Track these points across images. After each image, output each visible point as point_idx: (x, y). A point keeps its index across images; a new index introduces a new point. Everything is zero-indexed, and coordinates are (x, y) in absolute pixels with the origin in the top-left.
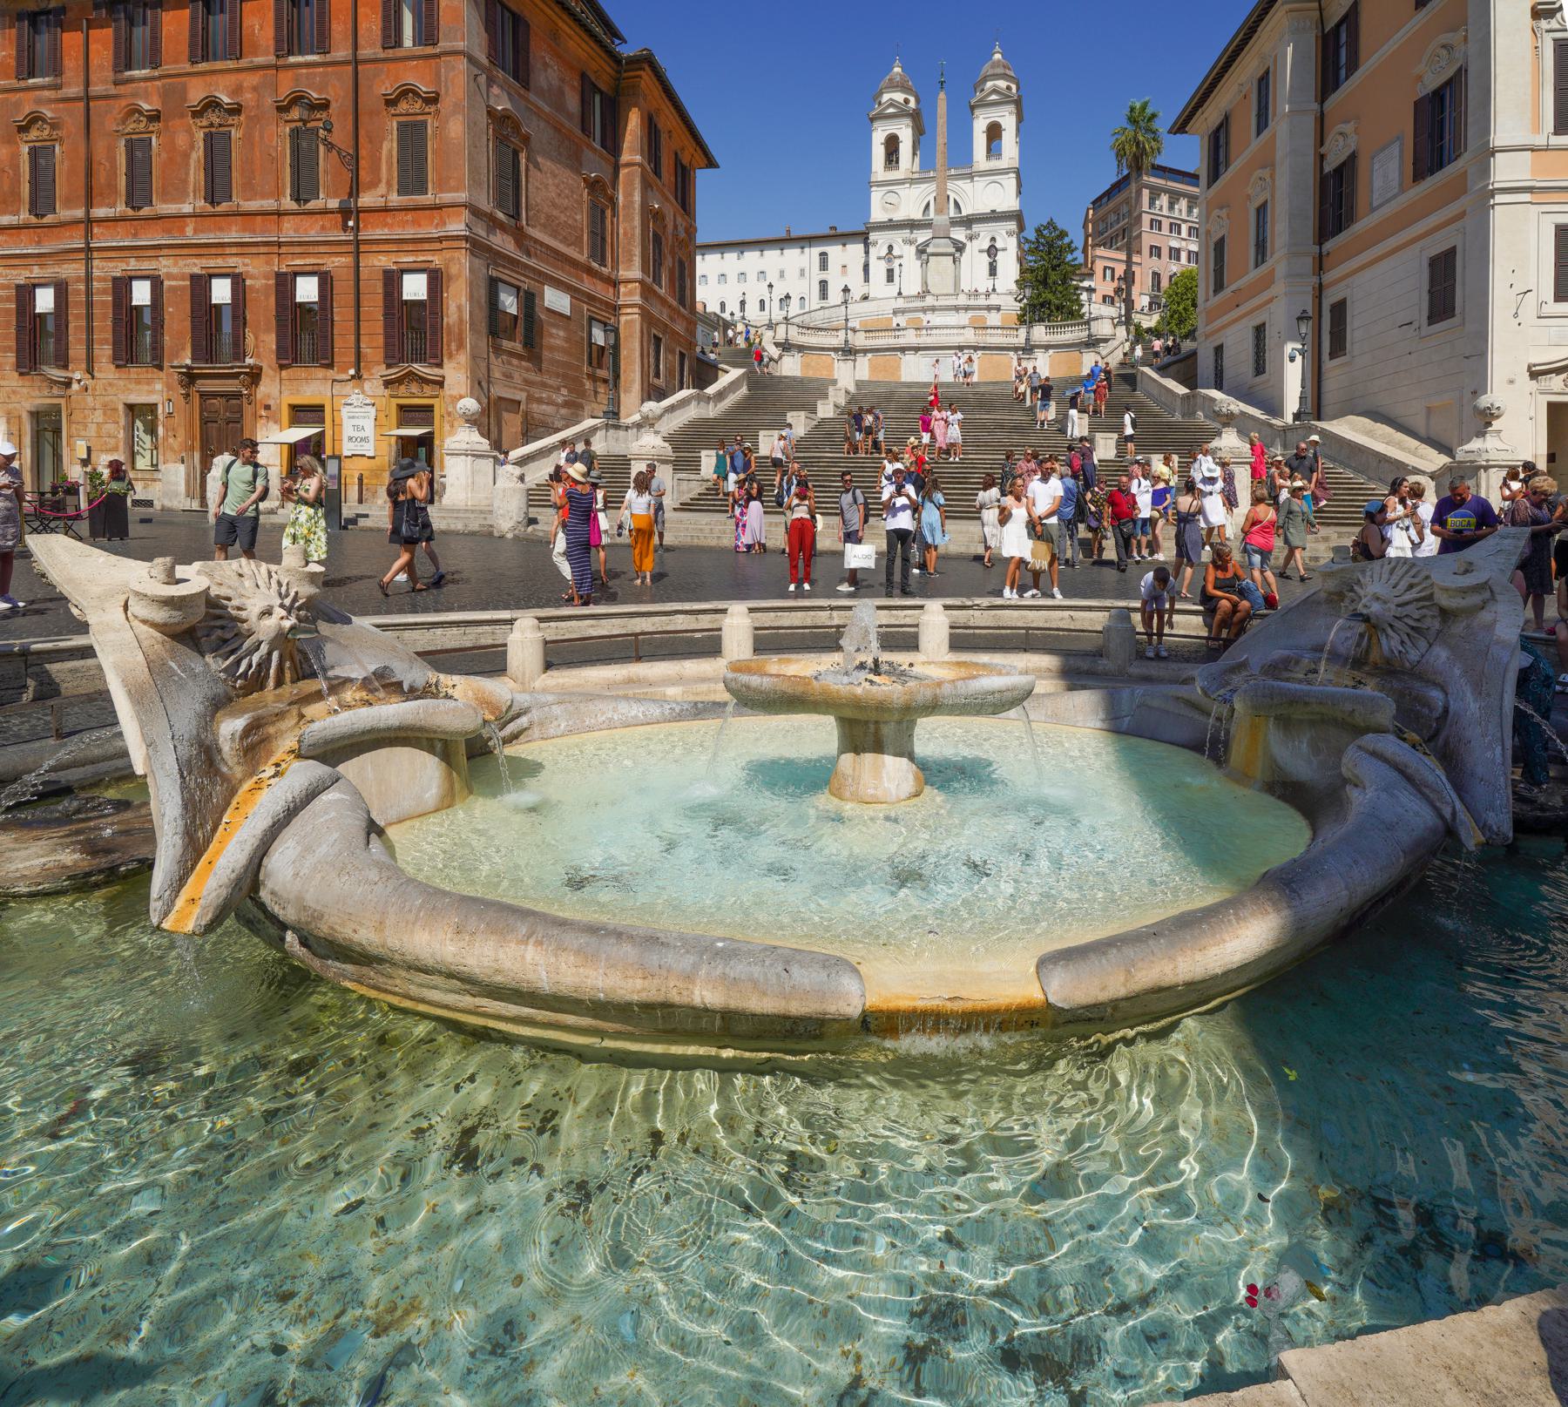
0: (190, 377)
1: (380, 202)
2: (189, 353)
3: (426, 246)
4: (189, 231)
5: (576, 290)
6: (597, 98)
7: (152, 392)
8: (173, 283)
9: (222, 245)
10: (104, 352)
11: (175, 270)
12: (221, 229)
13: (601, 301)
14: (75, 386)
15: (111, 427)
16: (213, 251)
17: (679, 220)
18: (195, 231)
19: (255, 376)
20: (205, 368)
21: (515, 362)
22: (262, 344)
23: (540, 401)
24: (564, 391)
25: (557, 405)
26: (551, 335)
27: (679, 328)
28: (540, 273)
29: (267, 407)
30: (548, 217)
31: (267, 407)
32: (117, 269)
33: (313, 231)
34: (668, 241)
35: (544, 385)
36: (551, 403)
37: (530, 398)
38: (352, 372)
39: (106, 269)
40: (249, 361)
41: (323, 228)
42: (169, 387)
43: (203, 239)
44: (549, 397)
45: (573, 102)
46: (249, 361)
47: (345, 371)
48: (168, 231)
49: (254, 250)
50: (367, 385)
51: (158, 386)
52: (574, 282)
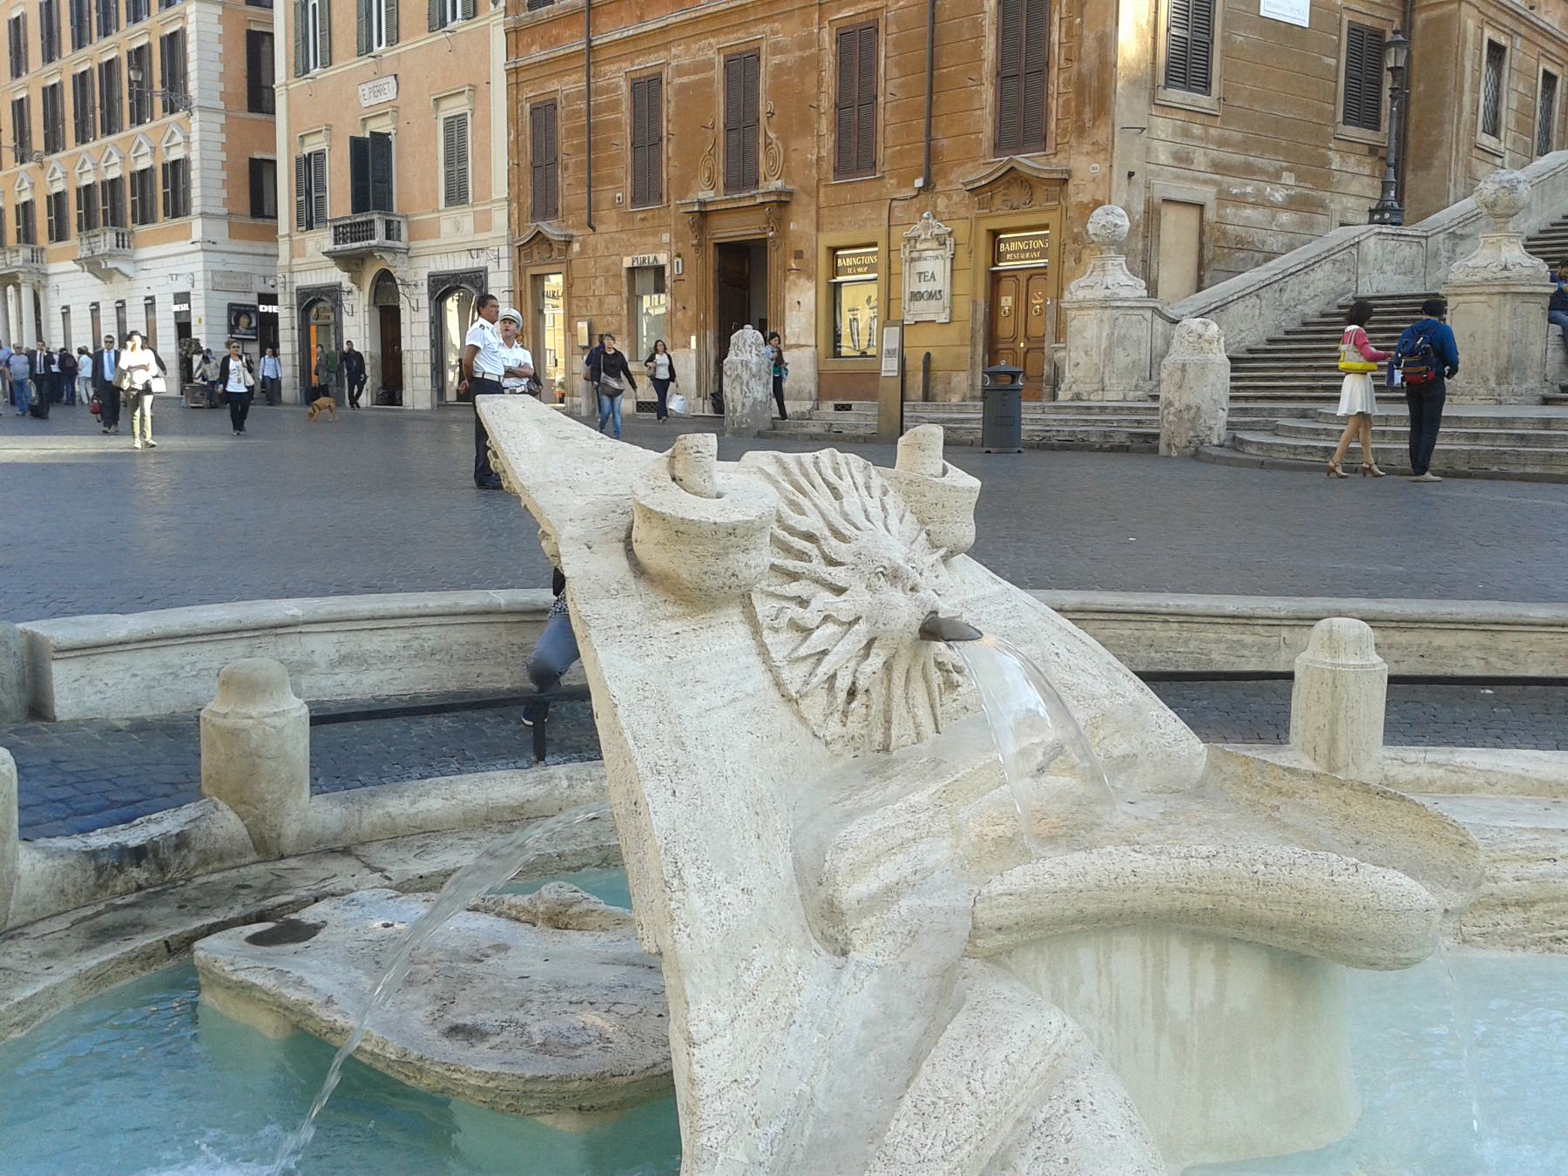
7: (658, 247)
8: (685, 79)
14: (576, 247)
19: (782, 203)
24: (1289, 178)
29: (799, 255)
31: (799, 255)
42: (678, 237)
46: (776, 184)
47: (906, 181)
50: (941, 203)
51: (666, 238)
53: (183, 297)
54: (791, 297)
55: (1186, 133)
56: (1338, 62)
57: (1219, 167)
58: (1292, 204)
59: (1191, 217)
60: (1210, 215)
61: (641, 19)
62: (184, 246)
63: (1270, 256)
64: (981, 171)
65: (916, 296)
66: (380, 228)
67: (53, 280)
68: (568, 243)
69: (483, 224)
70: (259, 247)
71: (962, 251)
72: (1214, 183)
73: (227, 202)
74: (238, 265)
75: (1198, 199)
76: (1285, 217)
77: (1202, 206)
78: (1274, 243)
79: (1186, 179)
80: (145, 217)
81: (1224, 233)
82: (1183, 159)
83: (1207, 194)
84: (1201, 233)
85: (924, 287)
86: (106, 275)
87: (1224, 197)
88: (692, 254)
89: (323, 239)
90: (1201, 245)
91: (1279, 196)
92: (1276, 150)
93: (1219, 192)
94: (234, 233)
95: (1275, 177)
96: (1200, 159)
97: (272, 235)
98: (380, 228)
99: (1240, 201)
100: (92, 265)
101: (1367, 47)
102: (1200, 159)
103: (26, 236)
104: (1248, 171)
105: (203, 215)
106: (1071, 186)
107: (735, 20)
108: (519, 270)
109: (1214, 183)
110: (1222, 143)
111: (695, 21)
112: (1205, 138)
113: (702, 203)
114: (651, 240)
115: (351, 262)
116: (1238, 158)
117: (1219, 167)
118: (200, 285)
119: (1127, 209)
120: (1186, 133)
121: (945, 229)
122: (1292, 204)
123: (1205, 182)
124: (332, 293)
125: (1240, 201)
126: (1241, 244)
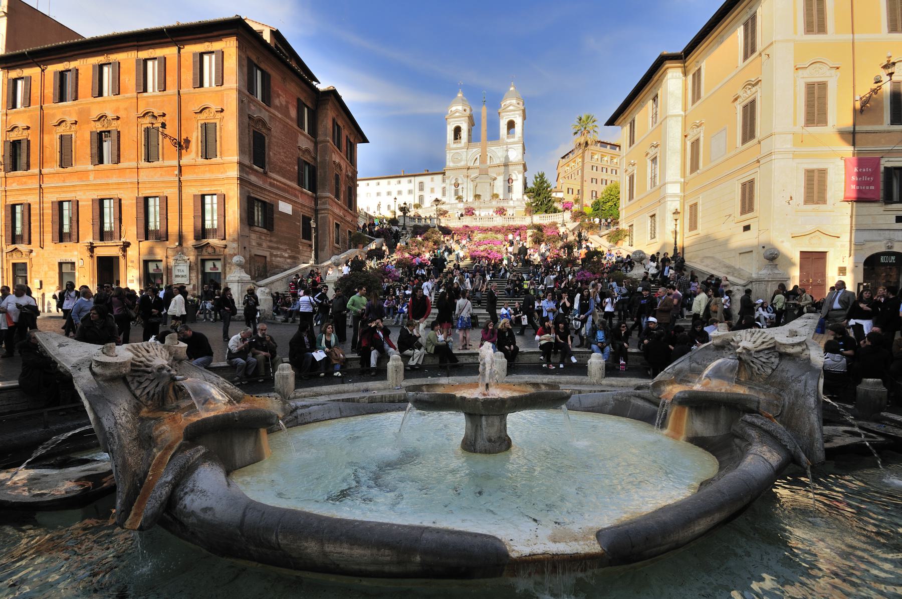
1: (193, 162)
3: (216, 183)
4: (91, 177)
5: (295, 202)
6: (306, 110)
9: (108, 184)
10: (48, 237)
11: (84, 197)
12: (108, 177)
13: (308, 207)
16: (104, 187)
17: (349, 168)
18: (95, 178)
22: (131, 231)
27: (349, 219)
28: (276, 194)
30: (281, 167)
32: (56, 197)
33: (157, 176)
34: (342, 178)
38: (177, 244)
39: (51, 197)
41: (161, 175)
43: (99, 182)
45: (293, 113)
48: (81, 179)
49: (125, 186)
52: (294, 199)
55: (260, 238)
56: (300, 224)
57: (270, 247)
58: (290, 257)
60: (268, 259)
63: (285, 270)
65: (177, 276)
76: (289, 261)
77: (265, 257)
78: (286, 267)
82: (260, 245)
83: (267, 254)
85: (180, 274)
87: (272, 255)
91: (287, 255)
92: (285, 244)
95: (285, 251)
99: (276, 256)
101: (306, 220)
102: (265, 245)
104: (278, 249)
110: (271, 241)
116: (276, 245)
117: (270, 247)
119: (244, 257)
120: (260, 238)
122: (290, 257)
125: (276, 256)
126: (277, 267)
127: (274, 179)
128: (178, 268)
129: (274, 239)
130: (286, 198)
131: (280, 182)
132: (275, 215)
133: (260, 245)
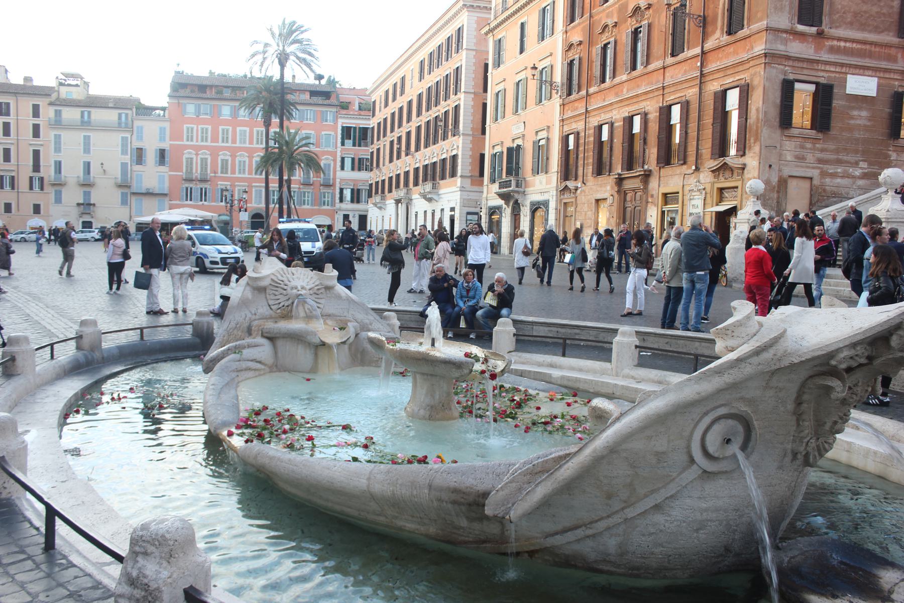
0: (620, 180)
2: (620, 167)
7: (605, 191)
14: (579, 191)
15: (589, 213)
20: (626, 174)
21: (809, 145)
23: (834, 175)
25: (854, 177)
26: (852, 118)
28: (842, 65)
35: (839, 162)
36: (846, 176)
37: (824, 174)
40: (646, 167)
42: (612, 188)
44: (845, 172)
46: (646, 167)
51: (609, 188)
53: (453, 209)
54: (649, 213)
55: (802, 147)
59: (806, 185)
60: (816, 182)
61: (604, 100)
62: (454, 189)
64: (714, 164)
66: (513, 183)
67: (414, 201)
68: (576, 190)
69: (549, 182)
70: (476, 188)
71: (708, 196)
72: (819, 168)
73: (471, 171)
74: (473, 196)
75: (809, 175)
77: (811, 179)
79: (802, 167)
80: (443, 177)
81: (824, 190)
83: (815, 173)
84: (811, 190)
86: (430, 200)
88: (616, 195)
89: (495, 187)
90: (811, 195)
93: (821, 172)
94: (472, 184)
96: (810, 158)
97: (481, 184)
98: (513, 183)
100: (424, 196)
102: (810, 158)
103: (406, 184)
105: (461, 176)
106: (746, 171)
107: (634, 100)
108: (559, 201)
109: (819, 168)
110: (822, 150)
111: (621, 101)
112: (814, 149)
113: (619, 175)
114: (603, 189)
115: (502, 196)
117: (820, 161)
118: (458, 204)
121: (702, 187)
123: (813, 168)
124: (499, 208)
127: (839, 39)
128: (693, 202)
129: (831, 146)
130: (856, 67)
131: (853, 41)
132: (837, 103)
133: (801, 158)
